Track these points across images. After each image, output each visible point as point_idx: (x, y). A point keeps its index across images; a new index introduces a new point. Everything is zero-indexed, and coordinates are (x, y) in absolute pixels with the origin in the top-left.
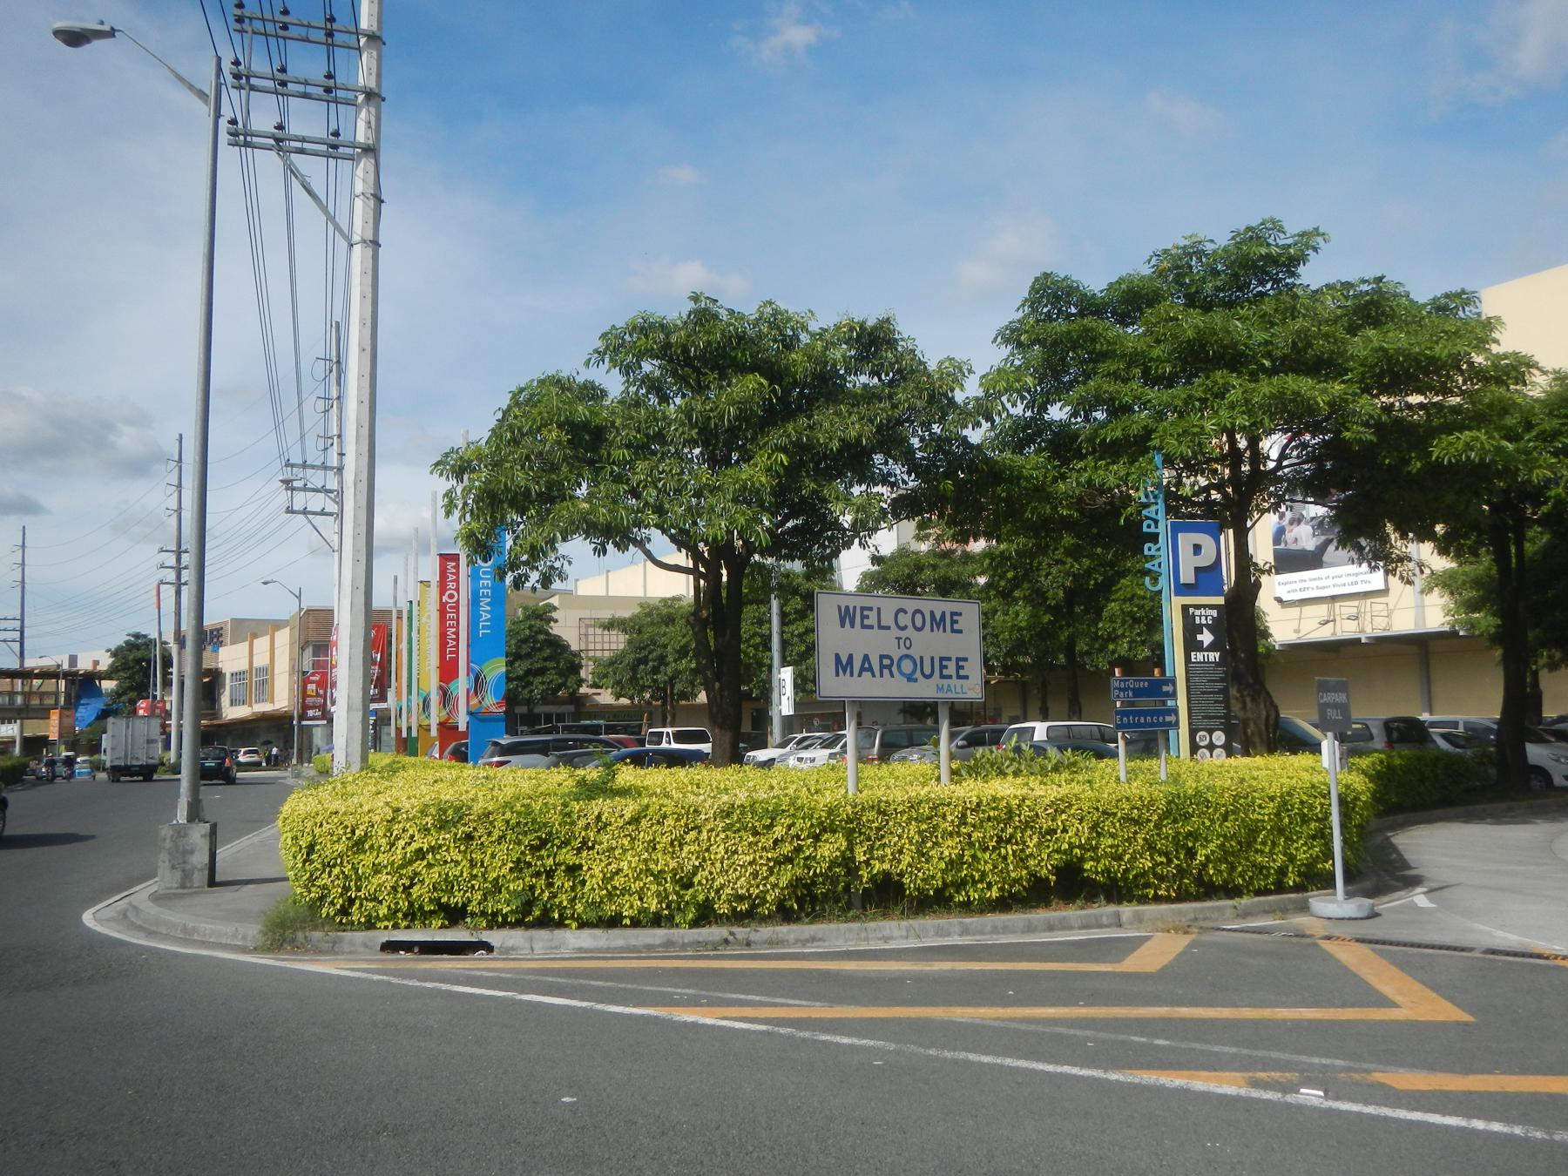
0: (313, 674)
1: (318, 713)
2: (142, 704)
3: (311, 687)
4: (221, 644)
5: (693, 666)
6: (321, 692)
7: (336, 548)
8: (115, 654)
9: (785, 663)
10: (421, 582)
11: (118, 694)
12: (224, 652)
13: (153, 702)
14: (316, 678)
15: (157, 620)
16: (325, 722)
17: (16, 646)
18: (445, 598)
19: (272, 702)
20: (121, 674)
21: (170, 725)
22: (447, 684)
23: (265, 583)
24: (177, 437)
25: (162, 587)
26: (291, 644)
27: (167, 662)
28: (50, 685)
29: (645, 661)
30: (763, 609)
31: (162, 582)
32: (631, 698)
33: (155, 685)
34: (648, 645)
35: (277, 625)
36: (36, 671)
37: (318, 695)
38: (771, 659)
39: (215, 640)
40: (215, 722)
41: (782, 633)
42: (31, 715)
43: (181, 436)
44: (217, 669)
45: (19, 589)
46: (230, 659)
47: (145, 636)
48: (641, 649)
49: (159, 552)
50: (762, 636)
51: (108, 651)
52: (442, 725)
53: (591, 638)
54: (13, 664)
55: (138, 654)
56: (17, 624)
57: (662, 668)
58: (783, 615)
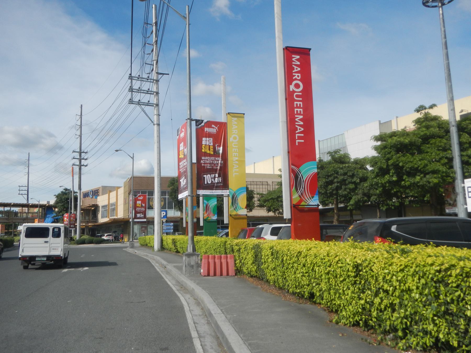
0: (140, 196)
1: (142, 216)
2: (66, 215)
3: (139, 203)
4: (98, 195)
5: (395, 179)
6: (144, 205)
7: (155, 123)
8: (57, 196)
9: (465, 177)
10: (229, 113)
11: (59, 212)
12: (99, 198)
13: (70, 214)
14: (141, 198)
15: (72, 181)
16: (145, 220)
17: (26, 196)
18: (292, 87)
19: (117, 216)
20: (60, 204)
21: (77, 225)
22: (298, 167)
23: (117, 151)
24: (80, 106)
25: (74, 166)
26: (124, 193)
27: (76, 199)
28: (36, 210)
29: (331, 183)
30: (444, 141)
31: (74, 165)
32: (274, 212)
33: (71, 209)
34: (332, 174)
35: (119, 187)
36: (30, 205)
37: (142, 206)
38: (455, 173)
39: (96, 194)
40: (96, 224)
41: (461, 156)
42: (28, 221)
43: (82, 105)
44: (96, 205)
45: (27, 175)
46: (102, 201)
47: (69, 190)
48: (329, 176)
49: (73, 152)
50: (446, 158)
51: (55, 195)
52: (295, 207)
53: (255, 186)
54: (25, 202)
55: (66, 196)
56: (26, 188)
57: (343, 187)
58: (461, 144)
